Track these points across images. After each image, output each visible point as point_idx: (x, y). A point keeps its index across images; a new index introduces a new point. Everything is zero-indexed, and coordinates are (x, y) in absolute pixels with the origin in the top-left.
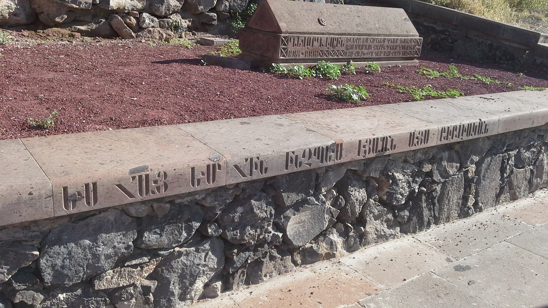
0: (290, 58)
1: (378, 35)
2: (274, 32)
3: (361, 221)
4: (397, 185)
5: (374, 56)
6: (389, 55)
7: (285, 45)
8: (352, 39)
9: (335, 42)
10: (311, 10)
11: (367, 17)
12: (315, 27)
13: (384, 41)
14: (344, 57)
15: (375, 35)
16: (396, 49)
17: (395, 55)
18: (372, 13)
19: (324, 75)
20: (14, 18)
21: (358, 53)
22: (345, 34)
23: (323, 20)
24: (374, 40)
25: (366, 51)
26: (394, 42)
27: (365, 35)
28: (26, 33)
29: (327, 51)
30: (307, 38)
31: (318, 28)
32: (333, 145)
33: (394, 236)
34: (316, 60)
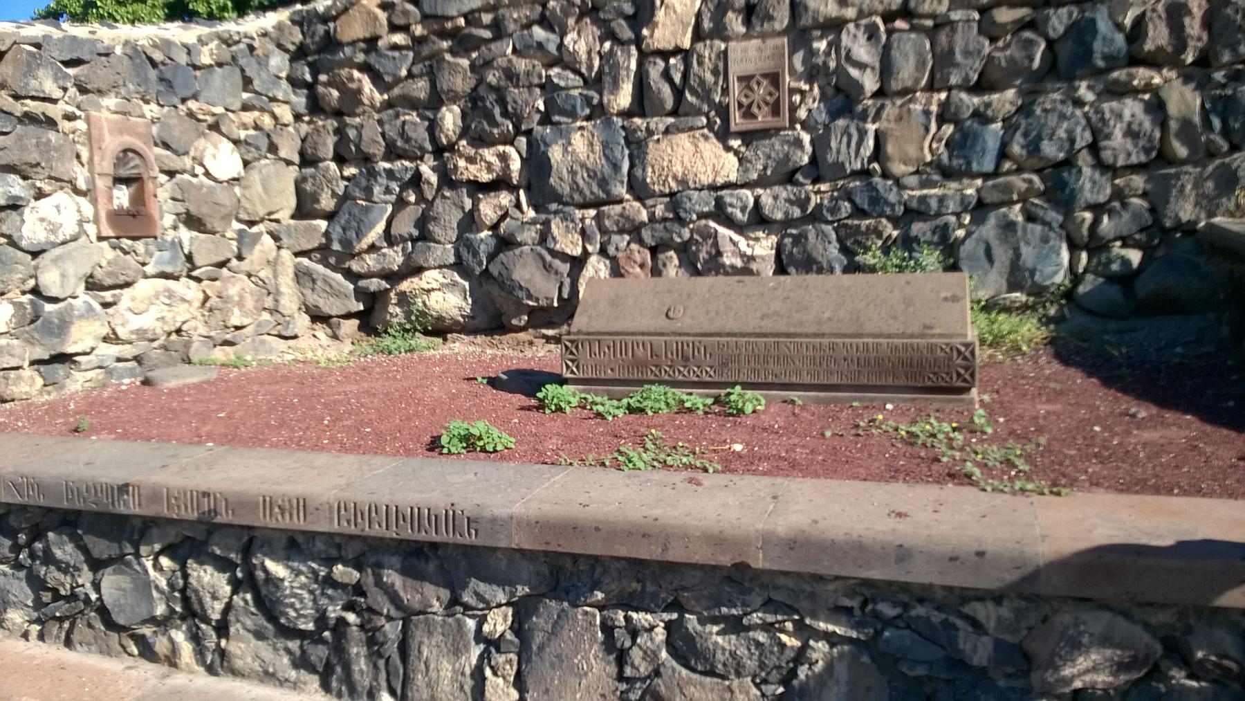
0: (586, 376)
1: (816, 335)
3: (222, 629)
4: (278, 587)
5: (807, 380)
7: (572, 353)
10: (670, 292)
14: (717, 379)
15: (807, 336)
20: (473, 322)
22: (719, 335)
25: (777, 369)
28: (480, 339)
29: (670, 367)
31: (661, 323)
32: (127, 485)
33: (295, 686)
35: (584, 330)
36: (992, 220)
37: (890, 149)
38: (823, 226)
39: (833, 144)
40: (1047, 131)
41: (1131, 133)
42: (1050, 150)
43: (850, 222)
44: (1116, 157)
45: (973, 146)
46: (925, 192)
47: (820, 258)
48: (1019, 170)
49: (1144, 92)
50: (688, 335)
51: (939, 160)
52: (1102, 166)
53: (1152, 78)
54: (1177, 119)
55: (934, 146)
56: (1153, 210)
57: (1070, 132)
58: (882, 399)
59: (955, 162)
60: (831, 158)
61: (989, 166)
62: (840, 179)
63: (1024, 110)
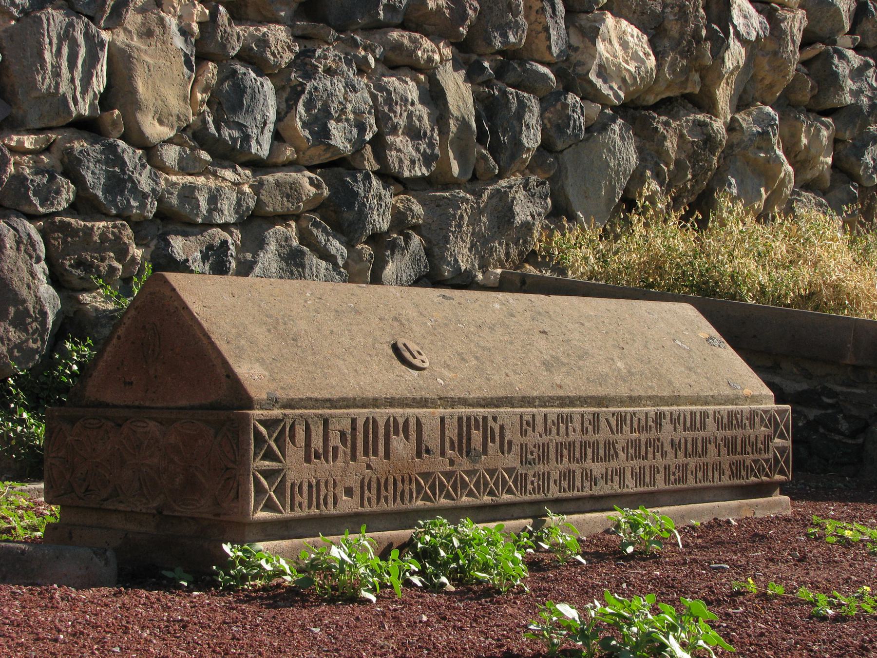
0: (298, 513)
1: (633, 400)
2: (214, 407)
5: (631, 486)
6: (683, 479)
7: (269, 455)
8: (539, 420)
9: (477, 436)
10: (358, 312)
11: (576, 335)
12: (385, 378)
13: (659, 425)
14: (518, 498)
15: (622, 402)
16: (705, 452)
17: (705, 477)
18: (589, 318)
19: (460, 577)
21: (569, 475)
22: (508, 401)
23: (411, 346)
24: (621, 419)
25: (598, 469)
26: (693, 427)
27: (585, 401)
30: (360, 423)
31: (404, 382)
34: (405, 519)
35: (281, 394)
36: (272, 247)
37: (141, 86)
38: (27, 223)
39: (47, 56)
40: (334, 107)
41: (414, 133)
42: (340, 137)
43: (73, 221)
44: (401, 161)
45: (250, 111)
46: (190, 179)
47: (24, 292)
48: (291, 165)
49: (421, 71)
50: (464, 402)
51: (204, 122)
52: (388, 177)
53: (433, 52)
54: (457, 119)
55: (199, 96)
56: (428, 252)
57: (358, 113)
58: (710, 511)
59: (226, 133)
60: (45, 83)
61: (264, 152)
62: (51, 129)
63: (304, 63)
